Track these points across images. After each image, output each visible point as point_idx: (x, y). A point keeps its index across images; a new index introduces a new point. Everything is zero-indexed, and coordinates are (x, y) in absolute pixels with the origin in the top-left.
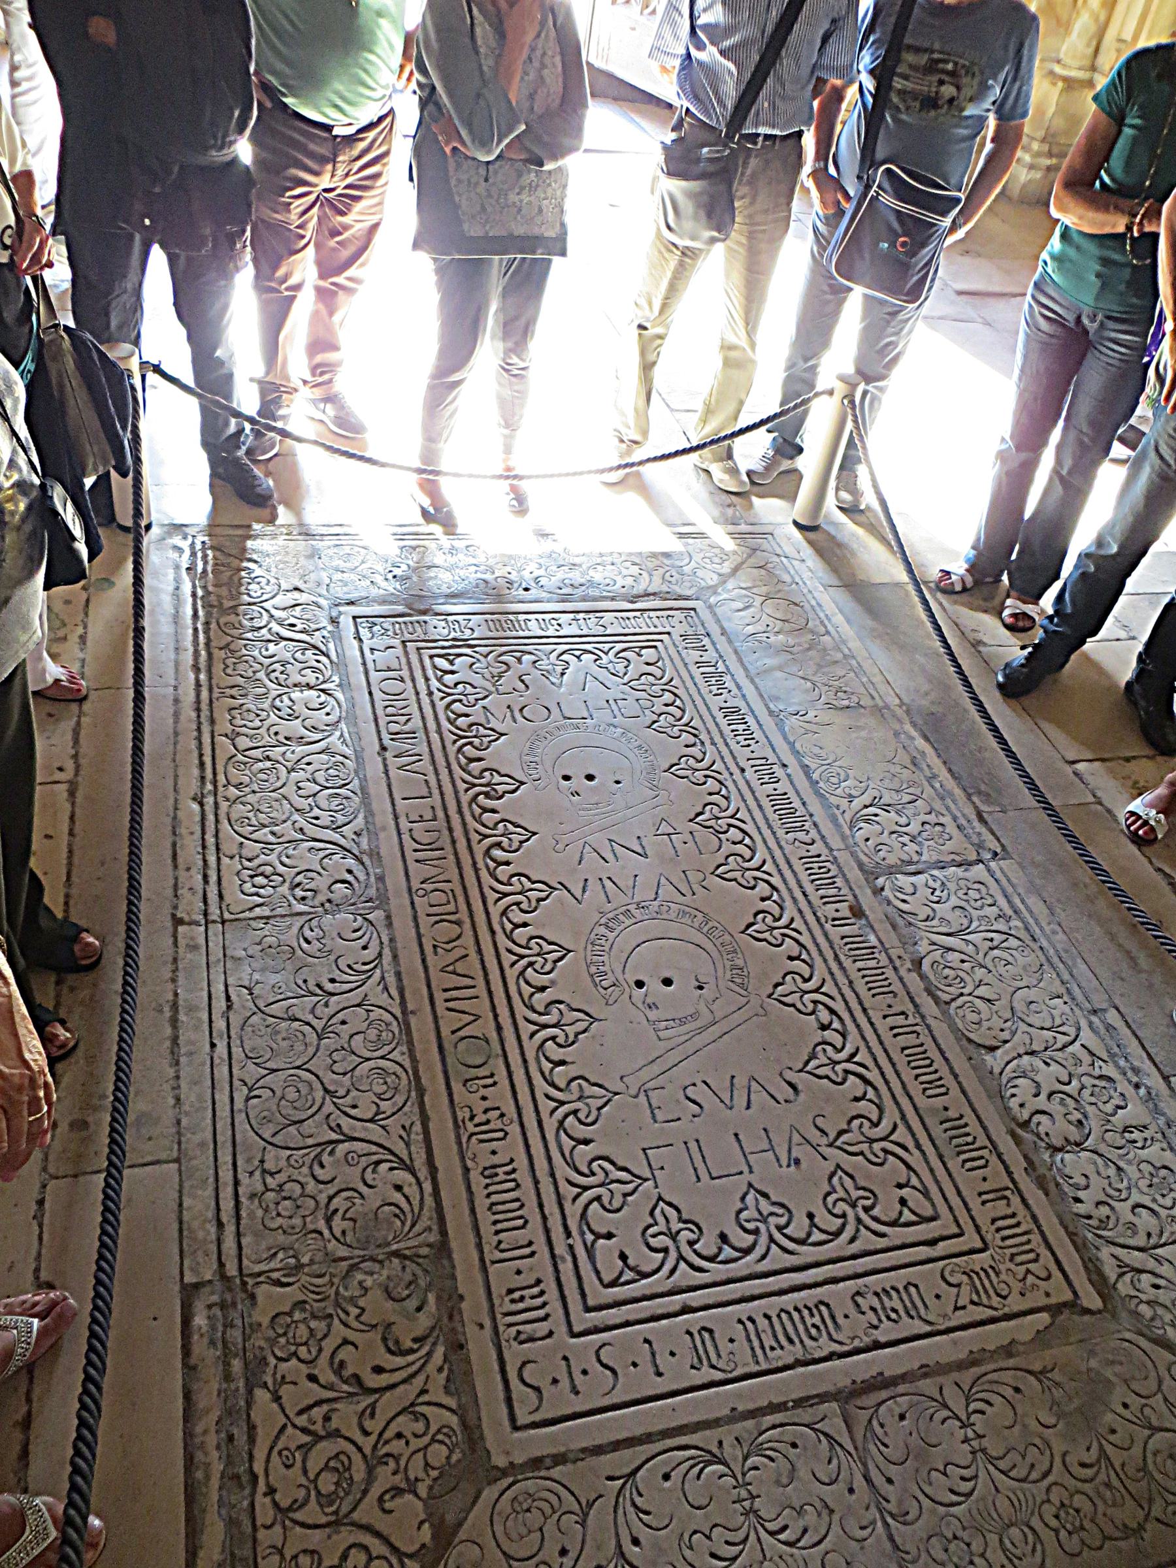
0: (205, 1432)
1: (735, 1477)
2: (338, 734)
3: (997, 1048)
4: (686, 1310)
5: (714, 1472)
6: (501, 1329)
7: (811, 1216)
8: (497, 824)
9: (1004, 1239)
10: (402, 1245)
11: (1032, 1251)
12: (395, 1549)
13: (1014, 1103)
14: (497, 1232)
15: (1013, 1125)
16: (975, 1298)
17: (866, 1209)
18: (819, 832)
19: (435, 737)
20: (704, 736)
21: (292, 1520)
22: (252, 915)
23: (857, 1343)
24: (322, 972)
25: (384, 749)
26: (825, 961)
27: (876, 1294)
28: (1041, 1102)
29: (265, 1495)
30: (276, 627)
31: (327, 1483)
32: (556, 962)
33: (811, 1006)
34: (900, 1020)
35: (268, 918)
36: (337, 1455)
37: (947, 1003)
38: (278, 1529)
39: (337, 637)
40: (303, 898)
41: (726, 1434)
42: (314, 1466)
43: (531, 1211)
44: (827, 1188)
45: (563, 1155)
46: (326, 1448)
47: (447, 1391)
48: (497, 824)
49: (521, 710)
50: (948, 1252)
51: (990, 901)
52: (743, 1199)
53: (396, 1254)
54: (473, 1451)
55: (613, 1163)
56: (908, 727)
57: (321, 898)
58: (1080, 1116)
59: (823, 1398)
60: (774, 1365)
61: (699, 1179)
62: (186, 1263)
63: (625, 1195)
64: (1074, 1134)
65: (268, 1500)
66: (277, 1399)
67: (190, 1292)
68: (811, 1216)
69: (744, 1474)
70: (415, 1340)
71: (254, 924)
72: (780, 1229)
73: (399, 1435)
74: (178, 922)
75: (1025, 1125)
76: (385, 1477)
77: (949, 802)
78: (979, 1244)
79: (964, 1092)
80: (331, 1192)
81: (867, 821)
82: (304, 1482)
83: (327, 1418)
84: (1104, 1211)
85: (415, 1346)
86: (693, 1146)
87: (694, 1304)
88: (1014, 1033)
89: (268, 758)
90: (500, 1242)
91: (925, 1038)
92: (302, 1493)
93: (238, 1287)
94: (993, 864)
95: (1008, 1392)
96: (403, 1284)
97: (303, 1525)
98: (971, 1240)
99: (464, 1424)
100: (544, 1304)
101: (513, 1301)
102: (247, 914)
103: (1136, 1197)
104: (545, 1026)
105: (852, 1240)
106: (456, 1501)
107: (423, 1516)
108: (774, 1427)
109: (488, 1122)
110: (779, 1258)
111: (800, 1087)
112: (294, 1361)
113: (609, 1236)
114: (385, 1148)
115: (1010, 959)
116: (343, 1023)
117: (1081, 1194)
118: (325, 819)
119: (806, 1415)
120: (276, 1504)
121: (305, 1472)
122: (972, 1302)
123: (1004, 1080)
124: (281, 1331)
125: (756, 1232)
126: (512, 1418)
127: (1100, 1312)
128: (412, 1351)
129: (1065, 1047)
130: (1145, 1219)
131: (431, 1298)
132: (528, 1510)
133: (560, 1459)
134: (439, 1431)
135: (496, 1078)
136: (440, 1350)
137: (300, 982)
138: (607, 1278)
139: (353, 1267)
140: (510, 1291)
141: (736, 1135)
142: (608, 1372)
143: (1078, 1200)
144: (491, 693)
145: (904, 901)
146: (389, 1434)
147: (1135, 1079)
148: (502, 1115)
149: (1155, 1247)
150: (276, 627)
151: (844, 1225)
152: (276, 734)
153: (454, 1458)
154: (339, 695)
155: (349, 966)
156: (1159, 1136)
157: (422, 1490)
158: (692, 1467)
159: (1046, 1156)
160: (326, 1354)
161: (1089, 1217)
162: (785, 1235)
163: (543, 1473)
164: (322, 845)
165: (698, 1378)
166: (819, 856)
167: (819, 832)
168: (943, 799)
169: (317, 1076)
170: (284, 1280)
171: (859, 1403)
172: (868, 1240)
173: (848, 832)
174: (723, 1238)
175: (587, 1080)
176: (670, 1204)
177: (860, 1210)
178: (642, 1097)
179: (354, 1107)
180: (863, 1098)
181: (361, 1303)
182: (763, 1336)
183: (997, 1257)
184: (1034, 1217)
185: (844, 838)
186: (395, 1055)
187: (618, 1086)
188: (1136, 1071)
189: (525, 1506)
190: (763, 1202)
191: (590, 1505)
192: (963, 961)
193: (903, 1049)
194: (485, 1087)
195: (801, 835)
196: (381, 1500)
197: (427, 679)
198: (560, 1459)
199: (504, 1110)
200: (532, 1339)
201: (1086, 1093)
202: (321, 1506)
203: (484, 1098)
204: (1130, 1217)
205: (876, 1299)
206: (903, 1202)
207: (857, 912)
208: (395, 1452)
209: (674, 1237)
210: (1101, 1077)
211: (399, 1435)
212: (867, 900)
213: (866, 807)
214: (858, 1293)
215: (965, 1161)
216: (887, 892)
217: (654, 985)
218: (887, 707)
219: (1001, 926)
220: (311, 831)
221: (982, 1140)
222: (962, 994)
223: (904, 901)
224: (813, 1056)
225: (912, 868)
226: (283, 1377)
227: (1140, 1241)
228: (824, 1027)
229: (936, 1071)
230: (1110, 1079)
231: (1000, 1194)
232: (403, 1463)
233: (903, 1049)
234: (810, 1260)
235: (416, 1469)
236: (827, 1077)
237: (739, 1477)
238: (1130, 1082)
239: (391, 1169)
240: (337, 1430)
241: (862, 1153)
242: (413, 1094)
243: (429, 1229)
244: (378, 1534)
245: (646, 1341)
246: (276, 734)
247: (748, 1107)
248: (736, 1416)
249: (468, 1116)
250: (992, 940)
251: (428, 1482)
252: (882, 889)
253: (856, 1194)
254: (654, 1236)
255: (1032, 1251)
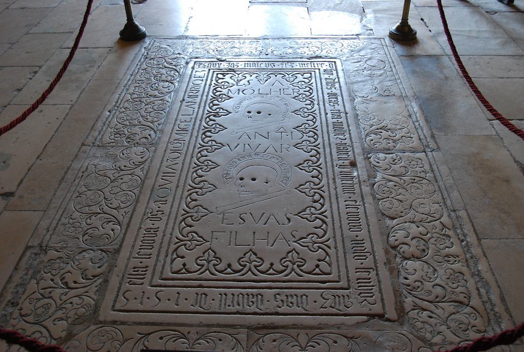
0: (10, 288)
1: (189, 345)
2: (169, 95)
3: (396, 218)
4: (200, 286)
5: (181, 341)
6: (125, 278)
7: (272, 264)
8: (213, 125)
9: (359, 287)
10: (103, 247)
11: (372, 293)
12: (51, 336)
13: (391, 239)
14: (140, 249)
15: (388, 247)
16: (333, 305)
17: (298, 266)
18: (350, 136)
19: (204, 97)
20: (316, 102)
21: (23, 320)
22: (109, 145)
23: (267, 311)
24: (122, 163)
25: (184, 100)
26: (328, 179)
27: (287, 296)
28: (408, 240)
29: (19, 310)
30: (166, 64)
31: (39, 311)
32: (211, 169)
33: (312, 194)
34: (353, 203)
35: (113, 146)
36: (47, 304)
37: (378, 199)
38: (17, 320)
39: (186, 67)
40: (129, 142)
41: (193, 330)
42: (39, 304)
43: (157, 246)
44: (285, 256)
45: (179, 229)
46: (46, 301)
47: (95, 293)
48: (213, 125)
49: (243, 91)
50: (329, 287)
51: (421, 166)
52: (245, 254)
53: (101, 250)
54: (94, 313)
55: (197, 234)
56: (414, 104)
57: (135, 142)
58: (424, 247)
59: (242, 326)
60: (227, 311)
61: (230, 245)
62: (31, 239)
63: (196, 245)
64: (418, 253)
65: (18, 311)
66: (38, 283)
67: (28, 248)
68: (272, 264)
69: (193, 345)
70: (92, 276)
71: (108, 148)
72: (255, 266)
73: (71, 303)
74: (83, 144)
75: (394, 248)
76: (59, 314)
77: (419, 130)
78: (346, 286)
79: (369, 232)
80: (89, 227)
81: (376, 134)
82: (33, 309)
83: (50, 293)
84: (417, 284)
85: (92, 278)
86: (234, 234)
87: (204, 285)
88: (407, 214)
89: (140, 101)
90: (139, 252)
91: (361, 210)
92: (30, 312)
93: (43, 249)
94: (429, 154)
95: (330, 341)
96: (98, 259)
97: (25, 321)
98: (343, 283)
99: (96, 306)
100: (145, 274)
101: (134, 271)
102: (107, 145)
103: (438, 281)
104: (195, 188)
105: (287, 275)
106: (79, 327)
107: (66, 329)
108: (215, 332)
109: (157, 215)
110: (249, 275)
111: (291, 220)
112: (50, 274)
113: (183, 257)
114: (115, 218)
115: (420, 187)
116: (122, 179)
117: (408, 276)
118: (150, 119)
119: (231, 331)
120: (20, 313)
121: (35, 307)
122: (331, 307)
123: (392, 230)
124: (50, 265)
125: (244, 266)
126: (113, 306)
127: (394, 321)
128: (91, 279)
129: (431, 222)
130: (439, 290)
131: (106, 265)
132: (103, 336)
133: (123, 323)
134: (85, 305)
135: (167, 202)
136: (100, 280)
137: (114, 166)
138: (174, 270)
139: (83, 251)
140: (135, 268)
141: (254, 232)
142: (158, 300)
143: (406, 278)
144: (234, 85)
145: (378, 162)
146: (69, 301)
147: (462, 238)
148: (163, 213)
149: (438, 302)
150: (166, 64)
151: (285, 270)
152: (147, 94)
153: (86, 314)
154: (177, 84)
155: (133, 163)
156: (464, 261)
157: (70, 320)
158: (173, 337)
159: (398, 260)
160: (60, 274)
161: (409, 286)
162: (257, 269)
163: (116, 326)
164: (144, 127)
165: (192, 309)
166: (346, 144)
167: (350, 136)
168: (417, 129)
169: (104, 193)
170: (59, 250)
171: (257, 332)
172: (293, 276)
173: (363, 137)
174: (229, 266)
175: (202, 207)
176: (213, 251)
177: (295, 266)
178: (222, 215)
179: (111, 204)
180: (320, 228)
181: (81, 261)
182: (228, 301)
183: (352, 292)
184: (379, 282)
185: (360, 138)
186: (135, 191)
187: (214, 210)
188: (465, 235)
189: (103, 334)
190: (253, 256)
191: (127, 340)
192: (395, 186)
193: (348, 213)
194: (161, 204)
195: (342, 137)
196: (54, 320)
197: (212, 80)
198: (123, 323)
199: (164, 212)
200: (134, 284)
201: (432, 240)
202: (34, 317)
203: (159, 207)
204: (431, 288)
205: (286, 297)
206: (317, 266)
207: (353, 164)
208: (67, 308)
209: (209, 262)
210: (444, 235)
211: (71, 303)
212: (360, 160)
213: (378, 129)
214: (278, 294)
215: (355, 256)
216: (371, 160)
217: (247, 180)
218: (406, 96)
219: (422, 175)
220: (143, 122)
221: (369, 249)
222: (388, 197)
223: (378, 162)
224: (304, 211)
225: (389, 152)
226: (43, 278)
227: (431, 298)
228: (315, 202)
229: (360, 223)
230: (448, 236)
231: (367, 270)
232: (67, 311)
233: (348, 213)
234: (263, 279)
235: (71, 314)
236: (307, 219)
237: (191, 345)
238: (459, 239)
239: (114, 224)
240: (51, 297)
241: (307, 246)
242: (135, 202)
243: (117, 244)
244: (48, 330)
245: (178, 293)
246: (147, 94)
247: (265, 224)
248: (200, 325)
249: (150, 212)
250: (414, 180)
251: (73, 319)
252: (370, 158)
253: (296, 260)
254: (200, 260)
255: (372, 293)
